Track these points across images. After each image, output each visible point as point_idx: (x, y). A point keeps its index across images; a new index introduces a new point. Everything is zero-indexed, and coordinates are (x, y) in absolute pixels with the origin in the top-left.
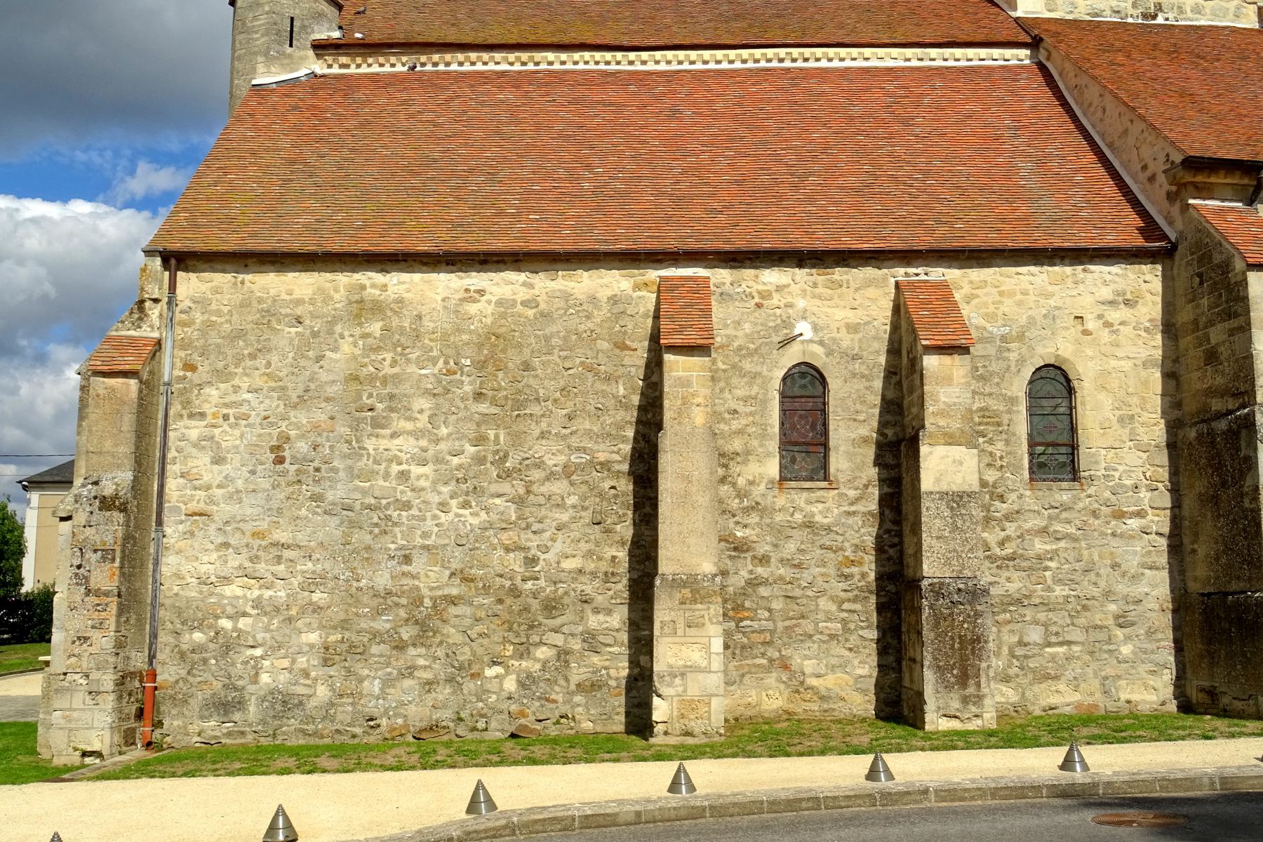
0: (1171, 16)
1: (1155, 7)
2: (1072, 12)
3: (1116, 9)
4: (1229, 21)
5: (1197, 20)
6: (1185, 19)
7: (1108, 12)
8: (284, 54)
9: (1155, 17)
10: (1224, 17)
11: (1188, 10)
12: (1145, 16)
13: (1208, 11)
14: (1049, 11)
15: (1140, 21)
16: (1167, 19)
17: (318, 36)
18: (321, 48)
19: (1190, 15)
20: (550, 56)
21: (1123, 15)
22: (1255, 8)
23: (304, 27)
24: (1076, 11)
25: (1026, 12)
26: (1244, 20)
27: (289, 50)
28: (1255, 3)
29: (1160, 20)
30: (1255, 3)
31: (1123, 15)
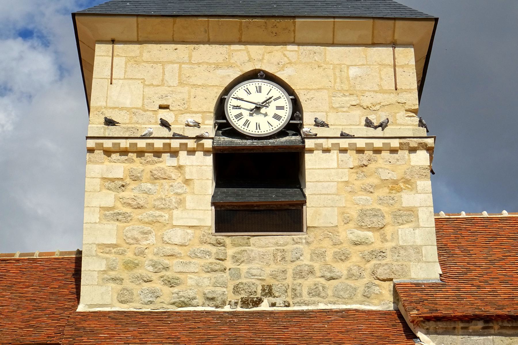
0: (278, 301)
1: (263, 290)
2: (151, 302)
3: (210, 296)
4: (356, 303)
5: (314, 303)
6: (299, 304)
7: (200, 300)
9: (258, 303)
10: (351, 298)
11: (305, 292)
12: (245, 303)
13: (330, 292)
14: (122, 302)
15: (239, 309)
16: (273, 305)
19: (306, 297)
21: (218, 303)
22: (389, 286)
24: (159, 300)
25: (90, 306)
26: (376, 301)
28: (391, 280)
29: (265, 306)
30: (391, 280)
31: (218, 303)
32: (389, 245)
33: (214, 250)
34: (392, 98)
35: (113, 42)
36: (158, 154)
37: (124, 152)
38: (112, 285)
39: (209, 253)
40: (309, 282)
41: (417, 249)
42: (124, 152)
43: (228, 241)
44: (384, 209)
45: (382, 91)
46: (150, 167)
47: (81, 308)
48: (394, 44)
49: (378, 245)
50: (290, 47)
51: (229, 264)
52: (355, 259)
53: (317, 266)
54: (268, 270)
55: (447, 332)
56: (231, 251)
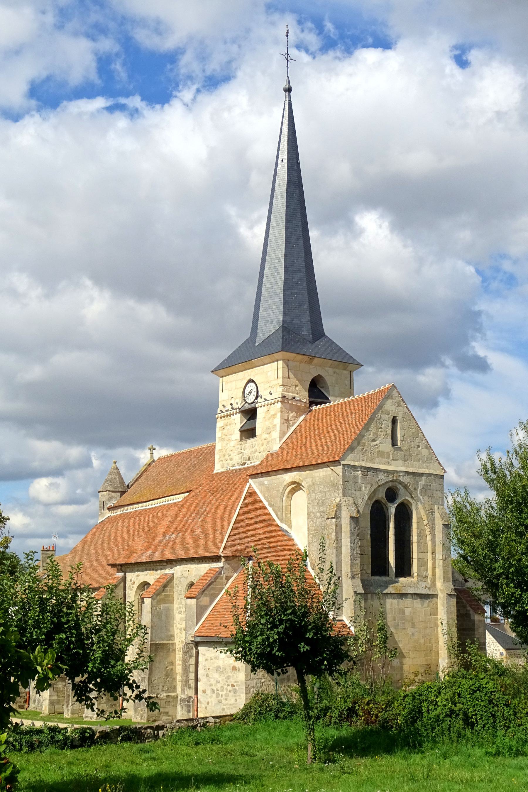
7: (236, 464)
8: (101, 513)
9: (244, 464)
17: (108, 506)
18: (109, 509)
20: (136, 506)
23: (106, 504)
27: (103, 511)
29: (246, 466)
32: (271, 439)
33: (239, 446)
34: (275, 382)
35: (223, 377)
36: (230, 415)
37: (224, 417)
38: (221, 463)
39: (238, 448)
40: (255, 455)
41: (275, 439)
42: (224, 417)
43: (243, 443)
44: (271, 426)
45: (275, 380)
46: (229, 421)
47: (215, 472)
48: (278, 361)
49: (269, 439)
50: (256, 368)
51: (242, 451)
52: (265, 445)
53: (258, 449)
54: (250, 451)
55: (255, 478)
56: (243, 446)
